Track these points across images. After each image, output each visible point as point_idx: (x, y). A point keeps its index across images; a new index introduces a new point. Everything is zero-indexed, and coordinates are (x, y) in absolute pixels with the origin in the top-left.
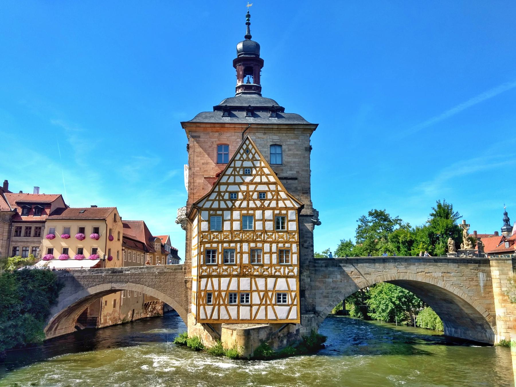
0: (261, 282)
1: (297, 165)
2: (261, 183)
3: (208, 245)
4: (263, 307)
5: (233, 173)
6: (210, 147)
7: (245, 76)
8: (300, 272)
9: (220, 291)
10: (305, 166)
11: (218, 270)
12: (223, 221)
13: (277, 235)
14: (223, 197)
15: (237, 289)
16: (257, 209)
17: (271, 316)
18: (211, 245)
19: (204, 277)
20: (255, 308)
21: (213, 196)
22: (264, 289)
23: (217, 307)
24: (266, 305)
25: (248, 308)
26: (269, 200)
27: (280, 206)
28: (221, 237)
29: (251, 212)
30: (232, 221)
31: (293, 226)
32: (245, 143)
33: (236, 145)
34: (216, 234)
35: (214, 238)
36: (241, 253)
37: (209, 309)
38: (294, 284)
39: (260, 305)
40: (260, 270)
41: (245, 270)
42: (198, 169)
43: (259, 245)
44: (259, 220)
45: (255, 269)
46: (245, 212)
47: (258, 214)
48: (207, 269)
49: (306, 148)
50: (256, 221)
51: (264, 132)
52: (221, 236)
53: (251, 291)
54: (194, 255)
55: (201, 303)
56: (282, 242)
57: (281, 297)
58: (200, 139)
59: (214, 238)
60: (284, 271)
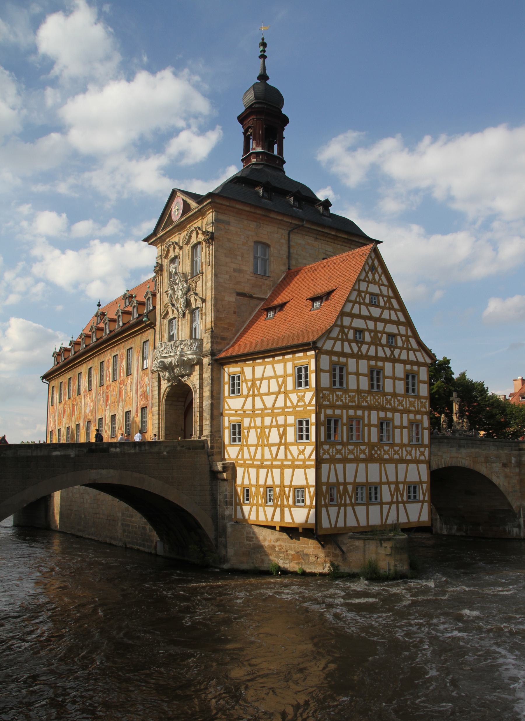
2: (391, 322)
3: (329, 412)
4: (394, 506)
5: (358, 300)
9: (345, 484)
11: (343, 451)
12: (348, 373)
14: (347, 335)
15: (365, 481)
16: (385, 359)
17: (403, 519)
18: (334, 412)
20: (386, 507)
22: (394, 480)
23: (342, 508)
24: (398, 503)
25: (378, 507)
28: (346, 399)
29: (380, 364)
30: (358, 374)
31: (424, 390)
34: (339, 393)
35: (337, 400)
37: (333, 511)
40: (390, 453)
41: (373, 452)
42: (227, 277)
43: (390, 415)
45: (384, 451)
46: (372, 363)
48: (329, 450)
50: (385, 377)
52: (346, 398)
55: (323, 503)
58: (231, 228)
59: (337, 400)
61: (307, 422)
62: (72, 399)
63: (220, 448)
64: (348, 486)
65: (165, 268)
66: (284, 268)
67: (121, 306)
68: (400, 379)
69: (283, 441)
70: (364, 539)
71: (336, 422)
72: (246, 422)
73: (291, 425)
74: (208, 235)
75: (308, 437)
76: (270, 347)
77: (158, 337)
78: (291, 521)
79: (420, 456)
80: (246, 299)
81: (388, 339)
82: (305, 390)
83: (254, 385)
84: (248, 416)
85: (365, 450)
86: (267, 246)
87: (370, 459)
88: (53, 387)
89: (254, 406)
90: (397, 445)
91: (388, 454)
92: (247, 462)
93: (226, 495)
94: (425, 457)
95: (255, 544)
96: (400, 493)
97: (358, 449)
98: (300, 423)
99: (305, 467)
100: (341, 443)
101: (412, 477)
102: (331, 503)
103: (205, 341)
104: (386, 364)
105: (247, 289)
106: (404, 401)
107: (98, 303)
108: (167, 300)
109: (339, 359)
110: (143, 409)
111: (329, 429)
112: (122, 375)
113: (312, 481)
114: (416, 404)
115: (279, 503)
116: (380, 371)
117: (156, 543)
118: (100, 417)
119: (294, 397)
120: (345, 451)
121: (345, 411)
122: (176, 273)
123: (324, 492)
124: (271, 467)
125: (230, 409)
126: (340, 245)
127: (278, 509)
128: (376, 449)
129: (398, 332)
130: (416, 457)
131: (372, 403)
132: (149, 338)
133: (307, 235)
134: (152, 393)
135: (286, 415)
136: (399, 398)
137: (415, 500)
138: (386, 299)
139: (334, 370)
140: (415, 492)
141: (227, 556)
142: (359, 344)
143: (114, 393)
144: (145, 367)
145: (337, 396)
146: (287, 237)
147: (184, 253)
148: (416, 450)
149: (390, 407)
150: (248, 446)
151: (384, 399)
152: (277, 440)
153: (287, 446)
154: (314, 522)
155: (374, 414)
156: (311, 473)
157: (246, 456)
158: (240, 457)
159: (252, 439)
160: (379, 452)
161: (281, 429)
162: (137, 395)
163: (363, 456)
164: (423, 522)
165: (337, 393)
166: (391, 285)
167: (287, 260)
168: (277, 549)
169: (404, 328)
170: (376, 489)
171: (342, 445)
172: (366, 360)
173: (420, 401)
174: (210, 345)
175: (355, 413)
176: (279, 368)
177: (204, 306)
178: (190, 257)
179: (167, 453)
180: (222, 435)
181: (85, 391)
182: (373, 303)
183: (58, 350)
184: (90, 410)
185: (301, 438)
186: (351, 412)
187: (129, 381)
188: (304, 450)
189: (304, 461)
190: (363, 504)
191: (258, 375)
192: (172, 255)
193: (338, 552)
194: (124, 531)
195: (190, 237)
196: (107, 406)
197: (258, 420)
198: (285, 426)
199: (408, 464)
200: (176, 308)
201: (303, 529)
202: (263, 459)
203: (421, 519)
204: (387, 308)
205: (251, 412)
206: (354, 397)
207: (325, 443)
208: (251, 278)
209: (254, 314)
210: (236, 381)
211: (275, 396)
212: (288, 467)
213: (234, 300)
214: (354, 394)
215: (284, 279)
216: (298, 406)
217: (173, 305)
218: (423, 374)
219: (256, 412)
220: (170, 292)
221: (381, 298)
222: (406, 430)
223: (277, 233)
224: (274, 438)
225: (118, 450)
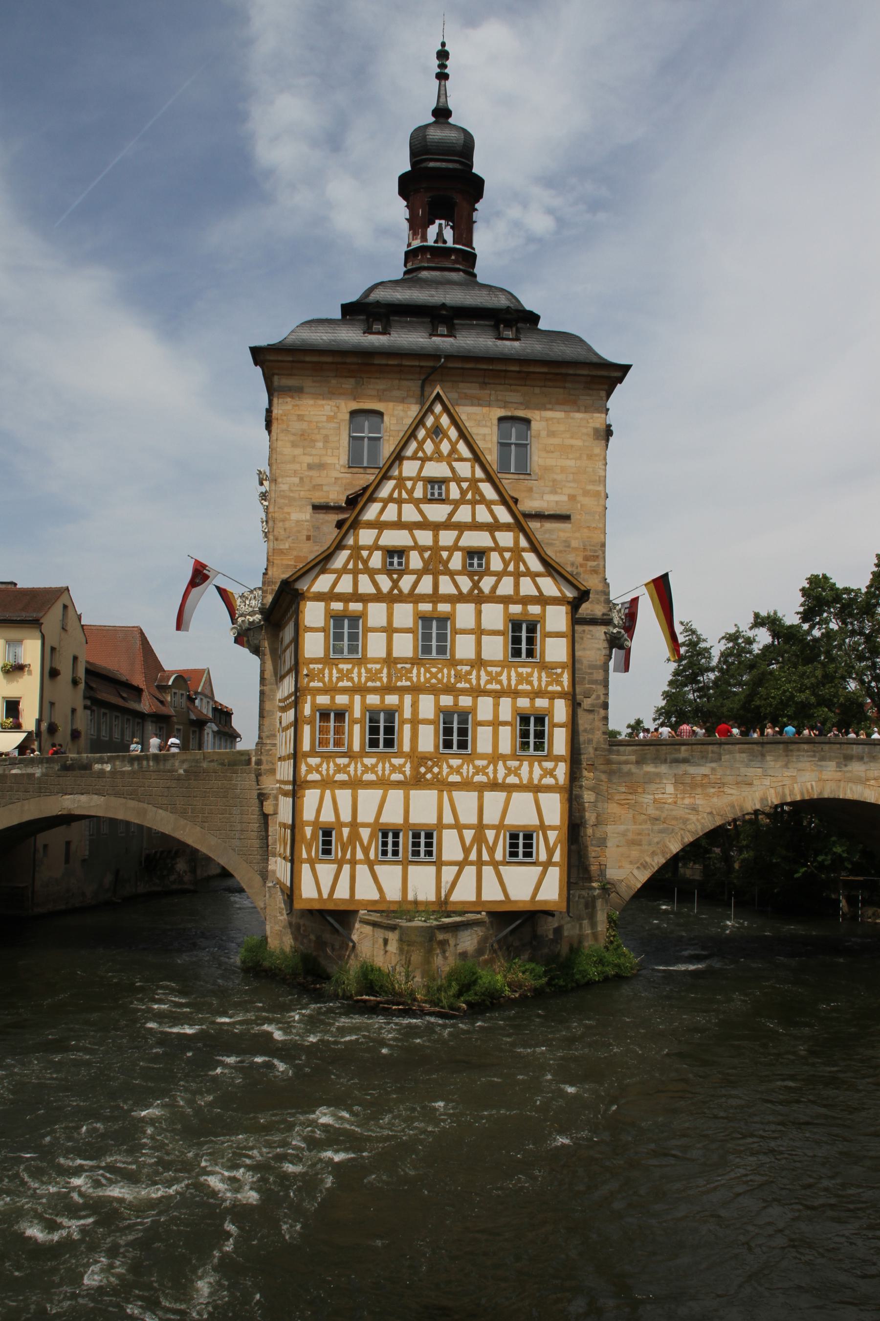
0: (466, 803)
1: (571, 477)
2: (475, 526)
3: (323, 700)
4: (470, 871)
6: (330, 419)
7: (433, 223)
8: (574, 775)
9: (354, 825)
10: (593, 482)
11: (351, 769)
12: (367, 630)
13: (513, 674)
14: (365, 562)
16: (460, 598)
18: (333, 699)
20: (449, 873)
21: (341, 559)
22: (474, 820)
24: (480, 863)
25: (432, 869)
27: (522, 593)
28: (359, 675)
32: (430, 410)
33: (401, 414)
34: (345, 667)
35: (339, 679)
36: (415, 722)
38: (553, 809)
39: (461, 865)
40: (464, 770)
41: (423, 770)
42: (296, 480)
43: (465, 701)
44: (464, 632)
47: (465, 614)
49: (596, 430)
50: (456, 632)
53: (440, 825)
54: (284, 724)
56: (525, 694)
57: (521, 844)
59: (339, 679)
60: (531, 772)
64: (361, 830)
71: (340, 716)
79: (542, 777)
87: (417, 782)
90: (482, 757)
91: (461, 774)
94: (556, 779)
96: (488, 847)
97: (387, 765)
104: (458, 606)
116: (444, 620)
126: (541, 387)
128: (430, 763)
129: (492, 545)
130: (531, 778)
131: (422, 679)
133: (462, 382)
136: (489, 669)
145: (340, 671)
146: (418, 392)
148: (531, 767)
149: (467, 685)
160: (436, 770)
163: (397, 777)
164: (546, 902)
165: (341, 666)
169: (510, 535)
171: (349, 757)
172: (410, 602)
175: (382, 700)
182: (436, 495)
186: (373, 699)
206: (380, 671)
213: (308, 517)
214: (378, 666)
221: (453, 486)
222: (509, 728)
223: (398, 389)
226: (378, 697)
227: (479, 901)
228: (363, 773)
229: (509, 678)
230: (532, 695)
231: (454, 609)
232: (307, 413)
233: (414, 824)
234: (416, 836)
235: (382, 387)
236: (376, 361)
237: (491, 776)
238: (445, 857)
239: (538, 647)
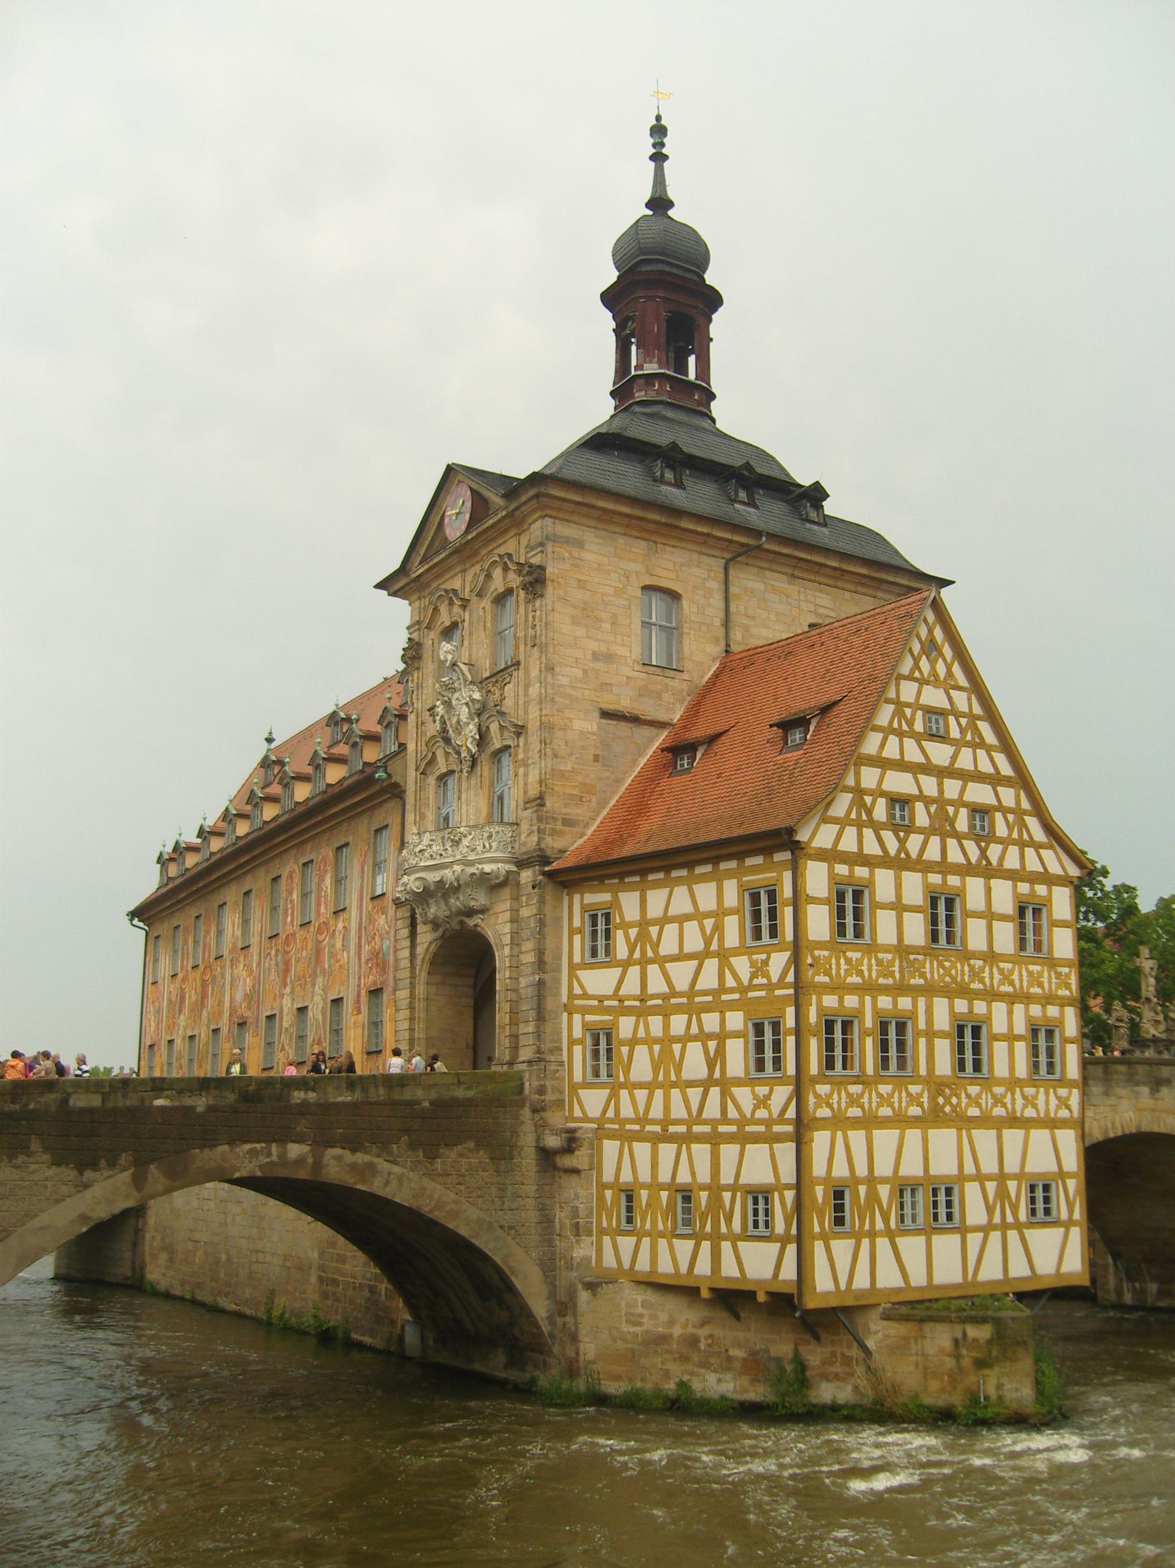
2: (980, 777)
3: (830, 1001)
4: (995, 1236)
5: (895, 725)
6: (619, 592)
9: (872, 1180)
11: (865, 1100)
13: (1024, 973)
14: (869, 812)
15: (921, 1173)
16: (968, 870)
17: (1019, 1269)
18: (841, 1000)
19: (823, 1123)
20: (974, 1239)
21: (842, 805)
22: (995, 1169)
23: (865, 1242)
24: (1004, 1227)
25: (956, 1238)
26: (1000, 841)
28: (870, 968)
29: (953, 880)
30: (899, 907)
34: (854, 955)
35: (848, 973)
37: (842, 1247)
40: (983, 1102)
41: (941, 1100)
42: (578, 673)
43: (980, 1007)
45: (968, 1096)
46: (935, 879)
48: (830, 1095)
50: (967, 914)
51: (790, 571)
55: (817, 1229)
58: (587, 556)
59: (848, 973)
60: (1047, 1102)
61: (776, 1027)
62: (202, 967)
63: (562, 1093)
64: (879, 1187)
65: (427, 653)
66: (717, 650)
67: (320, 743)
68: (1004, 918)
69: (717, 1075)
70: (922, 1320)
72: (626, 1026)
73: (737, 1035)
74: (529, 573)
75: (777, 1063)
76: (684, 842)
77: (410, 817)
78: (737, 1274)
79: (1058, 1107)
80: (624, 728)
81: (971, 819)
82: (768, 949)
83: (643, 936)
84: (629, 1011)
85: (920, 1095)
86: (674, 596)
87: (934, 1118)
88: (157, 937)
89: (644, 985)
90: (1000, 1082)
91: (978, 1105)
92: (628, 1127)
93: (575, 1210)
94: (1071, 1111)
95: (647, 1332)
97: (904, 1094)
98: (759, 1029)
99: (771, 1139)
100: (860, 1079)
101: (1041, 1162)
102: (838, 1229)
103: (524, 827)
104: (967, 878)
105: (625, 703)
106: (1016, 972)
107: (266, 735)
108: (433, 728)
109: (851, 871)
110: (375, 993)
111: (830, 1045)
112: (323, 910)
113: (788, 1174)
114: (1045, 980)
115: (708, 1228)
117: (403, 1327)
118: (268, 1013)
119: (742, 965)
120: (870, 1098)
121: (868, 999)
122: (454, 664)
123: (820, 1201)
124: (689, 1138)
125: (585, 996)
127: (706, 1245)
130: (1047, 1111)
132: (389, 821)
133: (770, 570)
134: (395, 956)
135: (722, 1008)
136: (1002, 965)
137: (1048, 1219)
138: (964, 721)
139: (841, 897)
140: (1047, 1200)
141: (577, 1361)
142: (902, 834)
143: (304, 953)
144: (379, 892)
145: (848, 961)
146: (722, 576)
147: (475, 617)
149: (981, 986)
150: (633, 1086)
151: (966, 968)
152: (703, 1073)
153: (726, 1085)
154: (795, 1278)
155: (941, 1005)
156: (786, 1152)
157: (627, 1111)
158: (610, 1113)
159: (641, 1066)
160: (954, 1100)
161: (712, 1045)
162: (360, 959)
163: (914, 1111)
164: (1070, 1275)
165: (849, 954)
166: (977, 688)
167: (723, 630)
168: (702, 1346)
169: (1011, 791)
170: (949, 1191)
171: (863, 1083)
172: (919, 871)
173: (1056, 973)
174: (536, 839)
175: (895, 1003)
176: (706, 894)
177: (521, 744)
178: (489, 625)
179: (431, 1103)
180: (565, 1058)
181: (234, 949)
183: (169, 848)
184: (246, 995)
185: (760, 1065)
186: (885, 1002)
187: (340, 925)
188: (768, 1097)
189: (768, 1123)
190: (918, 1232)
191: (655, 909)
192: (445, 619)
193: (854, 1352)
194: (325, 1295)
195: (489, 576)
196: (285, 985)
197: (656, 1022)
198: (722, 1037)
199: (1027, 1129)
200: (454, 749)
201: (769, 1293)
202: (666, 1122)
203: (1065, 1269)
204: (967, 744)
205: (637, 1003)
206: (891, 963)
207: (821, 1079)
208: (635, 674)
209: (643, 761)
210: (601, 926)
211: (694, 963)
212: (730, 1138)
213: (595, 728)
214: (889, 956)
215: (716, 676)
216: (751, 987)
217: (447, 740)
218: (1061, 903)
219: (649, 1003)
220: (440, 710)
221: (951, 719)
223: (698, 566)
224: (695, 1063)
225: (312, 1096)
226: (890, 999)
227: (1006, 1280)
228: (879, 1105)
229: (1020, 976)
230: (1043, 1001)
231: (963, 883)
232: (590, 579)
233: (935, 1176)
234: (935, 1192)
235: (678, 560)
236: (685, 524)
237: (1009, 1106)
238: (971, 1220)
239: (1044, 938)
